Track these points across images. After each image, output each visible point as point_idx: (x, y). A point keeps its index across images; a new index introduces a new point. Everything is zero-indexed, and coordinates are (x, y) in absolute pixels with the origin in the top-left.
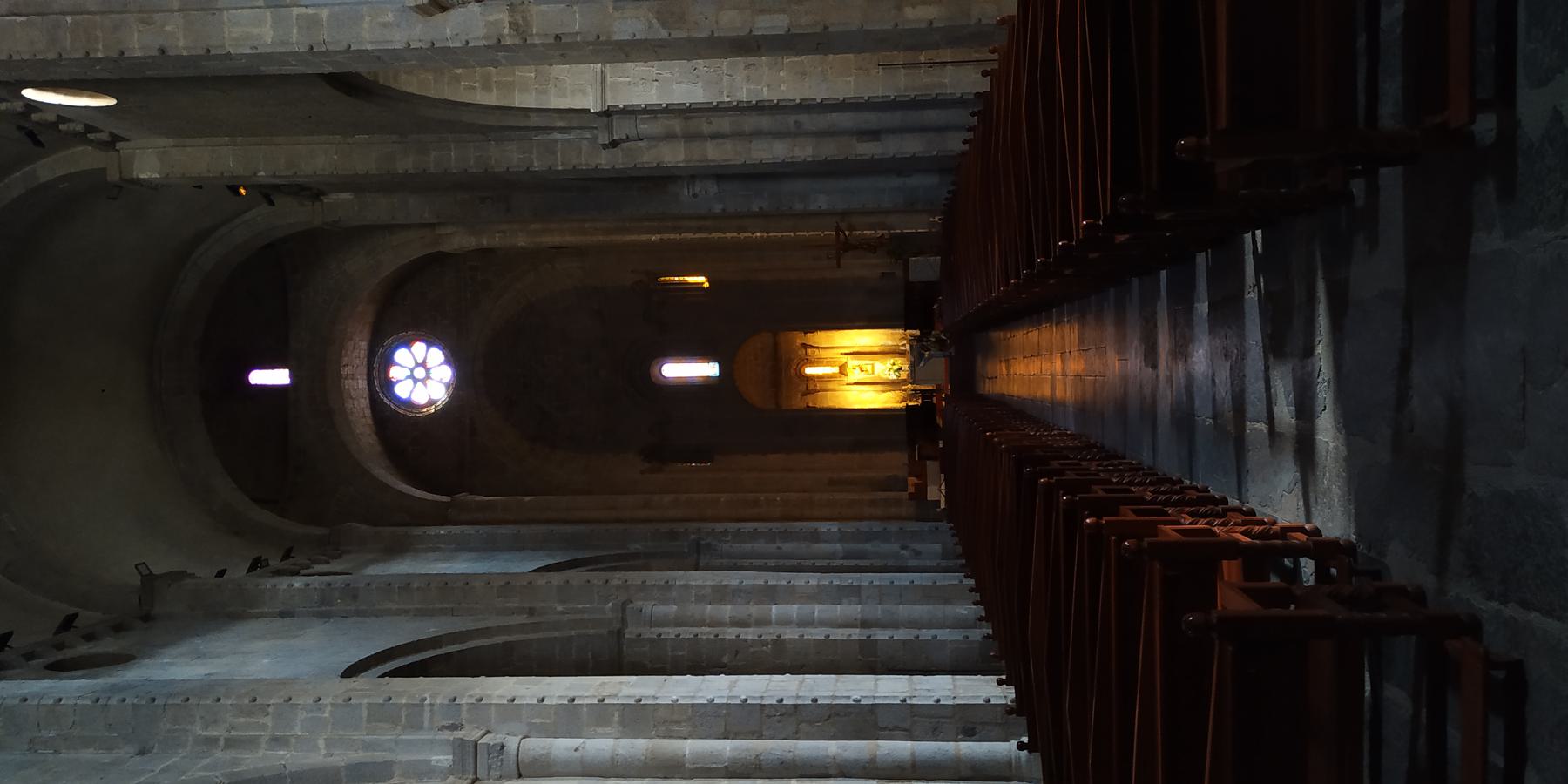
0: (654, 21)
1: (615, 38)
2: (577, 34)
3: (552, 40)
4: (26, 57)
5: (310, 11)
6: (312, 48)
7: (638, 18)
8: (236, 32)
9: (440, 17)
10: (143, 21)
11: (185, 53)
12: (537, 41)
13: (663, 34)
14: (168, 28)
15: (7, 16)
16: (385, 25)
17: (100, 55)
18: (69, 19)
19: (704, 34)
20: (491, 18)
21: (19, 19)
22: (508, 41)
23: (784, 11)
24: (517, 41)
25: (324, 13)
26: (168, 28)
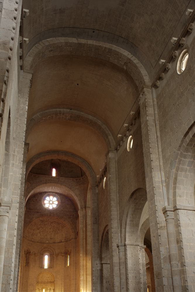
0: (164, 256)
1: (161, 248)
2: (161, 239)
3: (159, 234)
4: (149, 137)
5: (161, 188)
6: (154, 187)
7: (165, 252)
8: (157, 174)
9: (162, 212)
10: (157, 158)
11: (152, 164)
12: (159, 231)
13: (162, 258)
14: (156, 162)
15: (157, 135)
16: (160, 202)
17: (150, 150)
18: (157, 145)
19: (162, 267)
20: (163, 222)
21: (156, 137)
22: (158, 225)
23: (168, 284)
24: (158, 227)
25: (161, 190)
26: (156, 162)
